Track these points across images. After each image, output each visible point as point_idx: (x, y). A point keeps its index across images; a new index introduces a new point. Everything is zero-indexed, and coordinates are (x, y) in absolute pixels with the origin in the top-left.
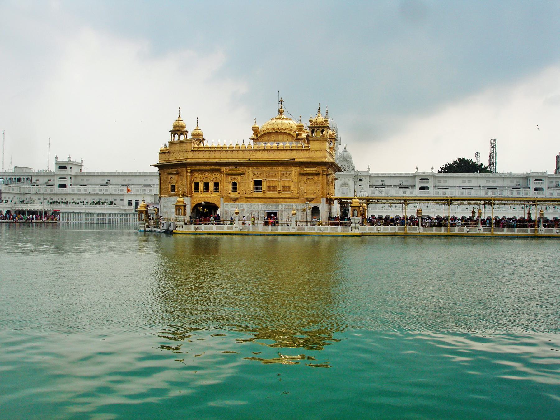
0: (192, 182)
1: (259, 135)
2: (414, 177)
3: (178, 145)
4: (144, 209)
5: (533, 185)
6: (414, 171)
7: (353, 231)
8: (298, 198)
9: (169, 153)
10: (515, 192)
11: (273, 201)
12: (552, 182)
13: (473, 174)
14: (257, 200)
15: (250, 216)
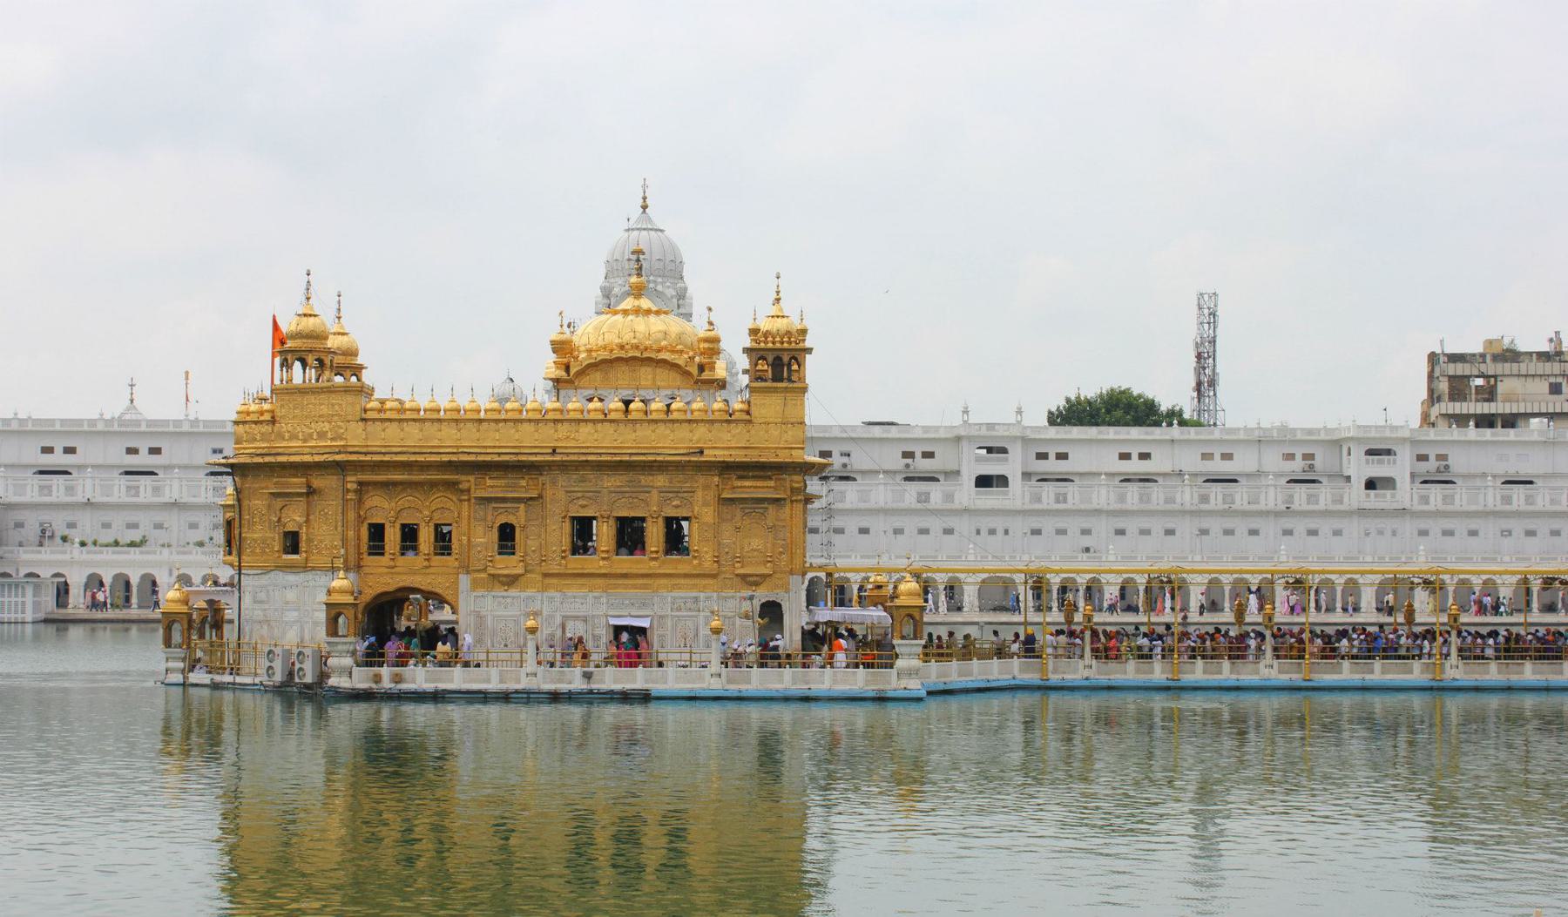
0: (360, 520)
1: (573, 369)
2: (958, 439)
3: (312, 398)
4: (184, 609)
5: (1360, 468)
6: (957, 420)
7: (903, 683)
8: (714, 576)
9: (273, 421)
10: (1301, 491)
11: (635, 587)
12: (1422, 458)
13: (1156, 430)
14: (580, 581)
15: (559, 633)
